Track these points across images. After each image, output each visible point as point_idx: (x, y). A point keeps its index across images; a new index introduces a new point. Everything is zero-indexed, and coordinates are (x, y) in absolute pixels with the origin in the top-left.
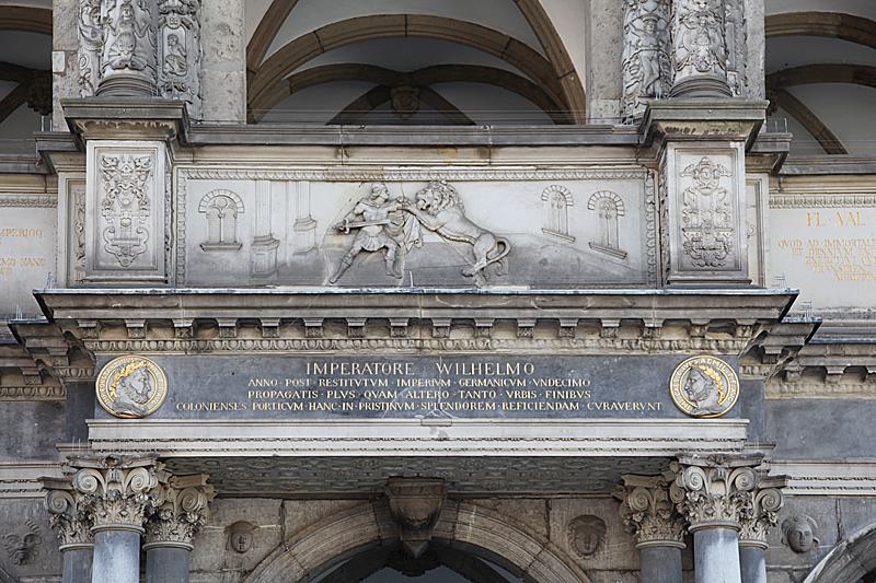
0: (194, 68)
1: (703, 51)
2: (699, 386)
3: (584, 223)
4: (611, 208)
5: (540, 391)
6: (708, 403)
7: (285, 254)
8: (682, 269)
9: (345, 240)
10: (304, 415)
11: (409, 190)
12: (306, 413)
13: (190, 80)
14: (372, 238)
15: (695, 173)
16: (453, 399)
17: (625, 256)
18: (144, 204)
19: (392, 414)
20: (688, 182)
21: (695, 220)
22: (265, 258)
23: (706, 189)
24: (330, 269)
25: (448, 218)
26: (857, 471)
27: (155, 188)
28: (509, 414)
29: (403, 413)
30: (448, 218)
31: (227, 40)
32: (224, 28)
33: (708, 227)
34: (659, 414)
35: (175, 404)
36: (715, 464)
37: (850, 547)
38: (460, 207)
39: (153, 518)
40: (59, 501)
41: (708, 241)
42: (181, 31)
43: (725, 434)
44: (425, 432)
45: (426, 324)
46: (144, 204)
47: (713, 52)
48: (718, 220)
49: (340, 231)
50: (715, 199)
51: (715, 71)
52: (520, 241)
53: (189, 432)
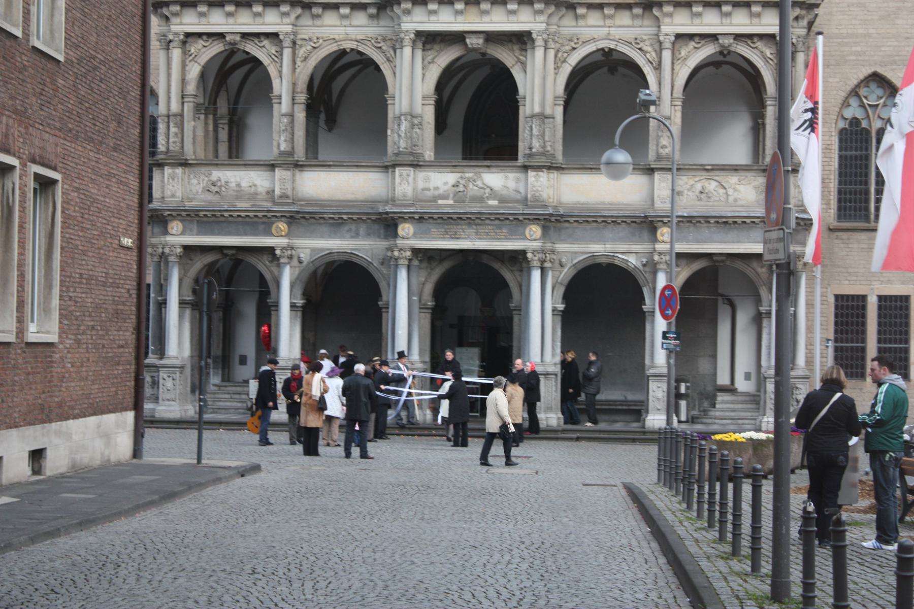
0: (421, 139)
1: (537, 145)
2: (532, 233)
3: (512, 184)
4: (518, 180)
5: (496, 233)
6: (533, 237)
7: (441, 192)
8: (531, 202)
9: (455, 188)
10: (443, 238)
11: (470, 175)
12: (444, 238)
13: (420, 143)
14: (461, 188)
15: (535, 177)
16: (477, 235)
17: (520, 193)
18: (408, 183)
19: (463, 238)
20: (533, 179)
21: (534, 189)
22: (436, 193)
23: (537, 181)
24: (451, 196)
25: (479, 183)
26: (576, 246)
27: (411, 179)
28: (489, 239)
29: (465, 238)
30: (479, 183)
31: (429, 126)
32: (429, 123)
33: (537, 191)
34: (523, 239)
35: (415, 235)
36: (534, 252)
37: (574, 265)
38: (482, 180)
39: (410, 260)
40: (389, 254)
41: (537, 194)
42: (418, 130)
43: (537, 245)
44: (470, 243)
45: (470, 218)
46: (408, 183)
47: (540, 146)
48: (540, 189)
49: (454, 186)
50: (539, 184)
51: (541, 150)
52: (496, 189)
53: (418, 242)
